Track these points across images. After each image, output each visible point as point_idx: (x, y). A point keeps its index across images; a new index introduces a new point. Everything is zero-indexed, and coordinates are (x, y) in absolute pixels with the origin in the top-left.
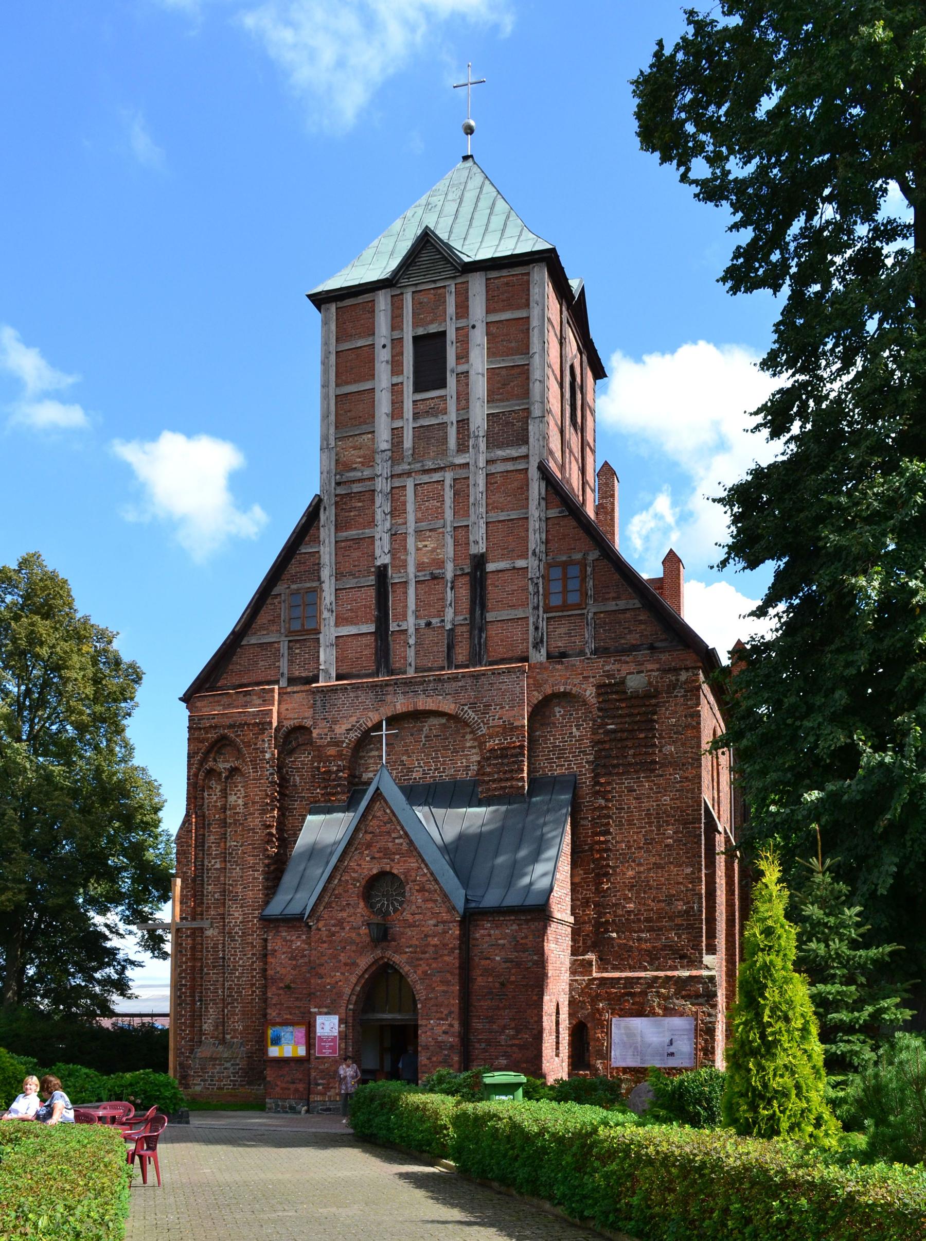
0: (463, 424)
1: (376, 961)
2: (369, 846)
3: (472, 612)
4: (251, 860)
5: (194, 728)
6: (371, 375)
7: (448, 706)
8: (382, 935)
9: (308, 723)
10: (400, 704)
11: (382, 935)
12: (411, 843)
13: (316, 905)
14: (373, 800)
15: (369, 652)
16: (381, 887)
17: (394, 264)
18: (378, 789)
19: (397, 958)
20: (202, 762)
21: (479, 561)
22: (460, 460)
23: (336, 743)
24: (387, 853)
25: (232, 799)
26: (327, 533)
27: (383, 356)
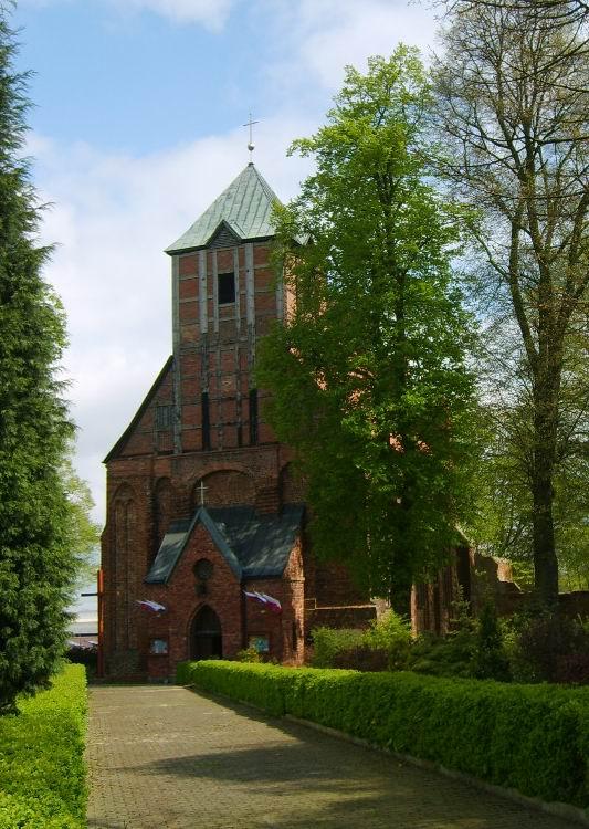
0: (244, 320)
1: (201, 604)
2: (195, 546)
3: (251, 417)
4: (140, 549)
5: (110, 478)
6: (197, 294)
7: (240, 468)
8: (203, 590)
9: (170, 475)
10: (216, 466)
11: (203, 590)
12: (215, 544)
13: (171, 576)
14: (197, 523)
15: (199, 438)
16: (202, 566)
17: (210, 234)
18: (199, 518)
19: (210, 603)
20: (115, 495)
21: (254, 393)
22: (242, 339)
23: (183, 486)
24: (205, 550)
25: (130, 516)
26: (177, 377)
27: (203, 284)
